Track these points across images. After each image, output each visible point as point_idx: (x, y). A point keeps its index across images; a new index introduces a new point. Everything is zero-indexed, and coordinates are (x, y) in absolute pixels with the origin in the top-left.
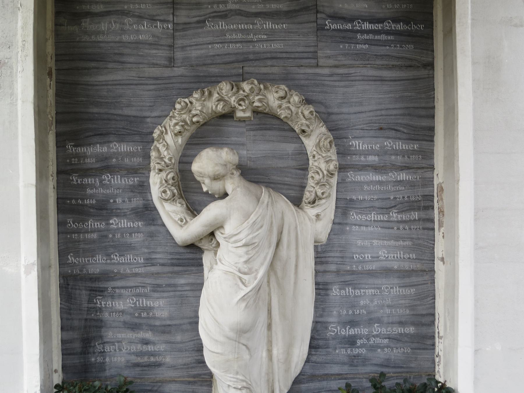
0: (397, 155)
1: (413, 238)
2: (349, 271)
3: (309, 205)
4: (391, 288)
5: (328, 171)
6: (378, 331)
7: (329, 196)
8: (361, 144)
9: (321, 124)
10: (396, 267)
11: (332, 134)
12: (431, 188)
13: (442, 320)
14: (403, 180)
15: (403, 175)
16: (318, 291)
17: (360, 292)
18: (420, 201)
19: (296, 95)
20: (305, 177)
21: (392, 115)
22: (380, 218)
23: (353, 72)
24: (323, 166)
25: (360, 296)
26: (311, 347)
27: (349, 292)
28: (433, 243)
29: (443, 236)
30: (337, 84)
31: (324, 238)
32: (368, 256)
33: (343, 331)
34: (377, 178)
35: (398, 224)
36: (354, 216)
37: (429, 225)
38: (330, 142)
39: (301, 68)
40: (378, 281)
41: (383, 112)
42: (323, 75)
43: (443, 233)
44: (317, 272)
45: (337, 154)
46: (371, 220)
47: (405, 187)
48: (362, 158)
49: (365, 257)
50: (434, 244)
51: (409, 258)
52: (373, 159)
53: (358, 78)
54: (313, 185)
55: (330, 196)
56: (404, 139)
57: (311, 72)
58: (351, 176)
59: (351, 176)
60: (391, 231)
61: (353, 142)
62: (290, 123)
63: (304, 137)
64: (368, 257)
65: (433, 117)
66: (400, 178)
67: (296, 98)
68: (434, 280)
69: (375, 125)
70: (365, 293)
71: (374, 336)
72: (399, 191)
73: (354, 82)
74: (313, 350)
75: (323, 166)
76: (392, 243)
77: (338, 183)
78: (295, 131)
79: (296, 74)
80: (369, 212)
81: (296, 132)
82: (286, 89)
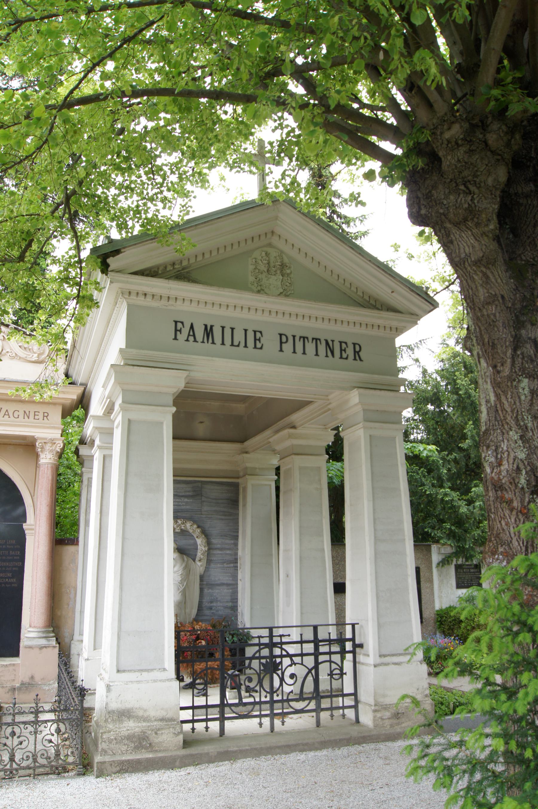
24: (203, 549)
26: (198, 610)
31: (202, 573)
32: (217, 579)
34: (220, 552)
36: (212, 565)
44: (200, 584)
52: (219, 546)
67: (195, 526)
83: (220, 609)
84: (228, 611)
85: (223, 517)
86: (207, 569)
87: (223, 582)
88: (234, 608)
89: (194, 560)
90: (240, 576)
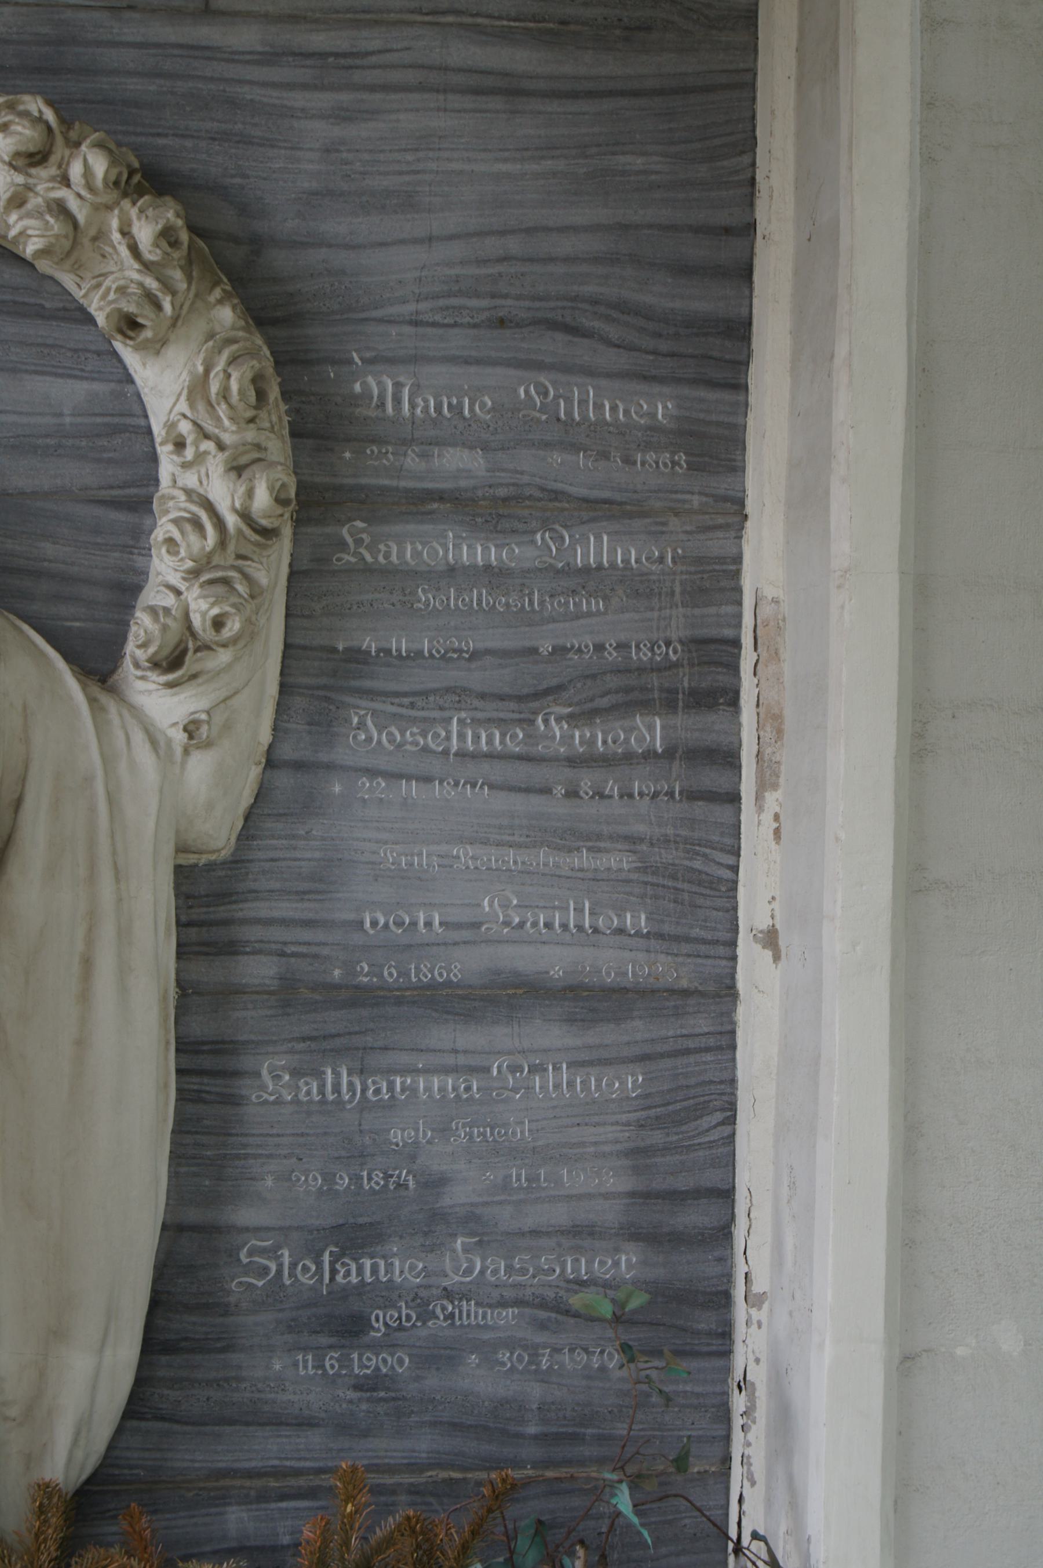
0: (575, 448)
1: (632, 840)
2: (337, 987)
3: (153, 676)
4: (533, 1069)
5: (245, 515)
6: (469, 1271)
7: (250, 634)
8: (406, 391)
9: (217, 293)
10: (557, 972)
11: (270, 343)
12: (729, 609)
13: (763, 1216)
14: (600, 567)
15: (598, 538)
16: (194, 1083)
17: (391, 1088)
18: (676, 665)
19: (100, 145)
20: (137, 542)
21: (551, 259)
22: (490, 741)
23: (376, 44)
24: (222, 492)
25: (392, 1104)
26: (154, 1344)
27: (337, 1088)
28: (730, 860)
29: (777, 832)
30: (298, 99)
33: (306, 1269)
34: (477, 552)
35: (568, 772)
36: (367, 733)
37: (712, 778)
38: (258, 381)
39: (128, 14)
40: (470, 1037)
41: (514, 245)
42: (233, 57)
43: (777, 817)
45: (293, 434)
46: (446, 752)
47: (606, 598)
48: (411, 461)
49: (414, 924)
50: (735, 869)
51: (621, 931)
52: (459, 464)
53: (395, 77)
54: (175, 579)
55: (253, 636)
56: (609, 375)
57: (173, 39)
58: (359, 542)
59: (359, 542)
60: (536, 801)
61: (370, 379)
62: (68, 280)
63: (136, 349)
64: (428, 924)
65: (746, 273)
66: (586, 555)
67: (91, 163)
68: (733, 1033)
69: (474, 303)
70: (414, 1090)
71: (448, 1294)
72: (578, 616)
73: (378, 96)
74: (164, 1359)
75: (222, 492)
76: (544, 858)
77: (292, 575)
78: (91, 320)
79: (99, 44)
80: (436, 714)
81: (95, 324)
82: (50, 115)
83: (491, 1334)
84: (587, 1366)
85: (521, 59)
86: (289, 780)
87: (523, 959)
88: (685, 1316)
89: (97, 662)
90: (760, 891)
